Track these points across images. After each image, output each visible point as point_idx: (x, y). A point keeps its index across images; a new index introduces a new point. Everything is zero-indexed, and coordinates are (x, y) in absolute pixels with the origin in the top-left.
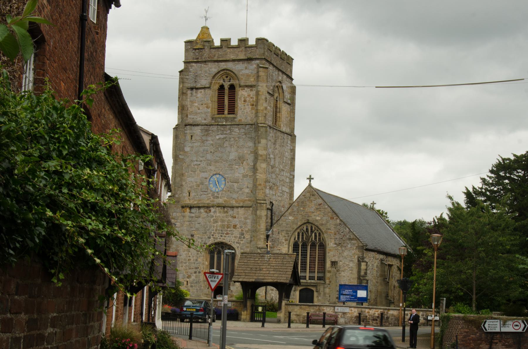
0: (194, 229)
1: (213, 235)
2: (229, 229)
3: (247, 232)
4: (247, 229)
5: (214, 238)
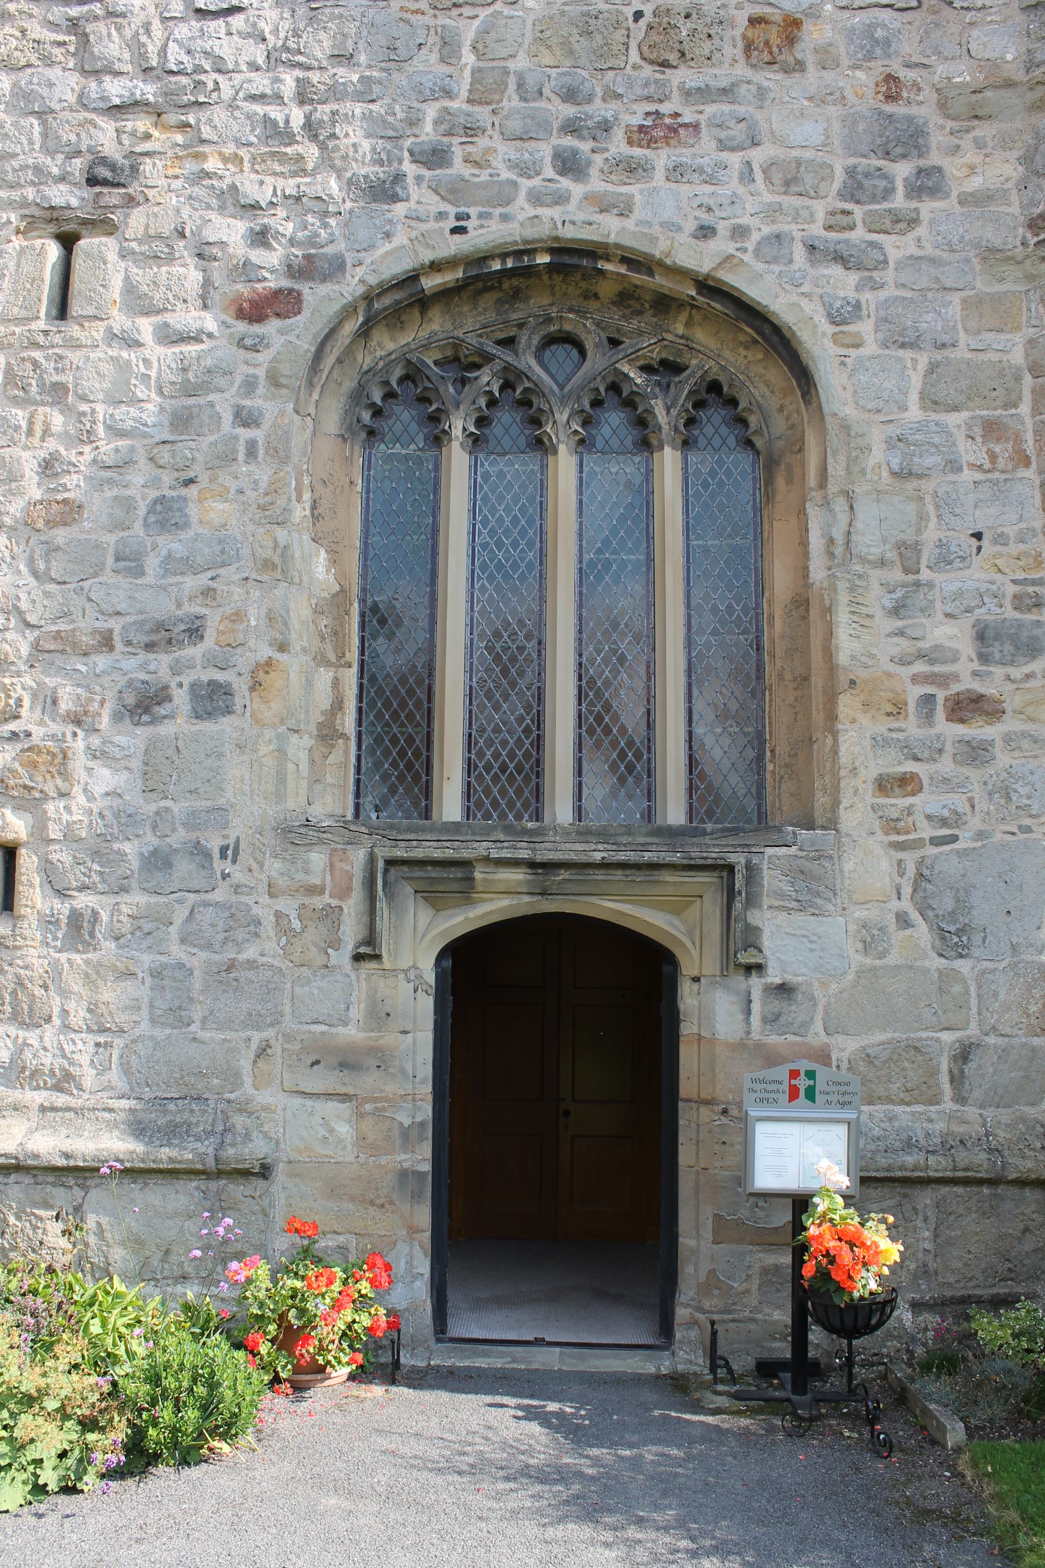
0: (148, 91)
1: (434, 157)
2: (681, 76)
3: (970, 110)
4: (962, 74)
5: (452, 192)
